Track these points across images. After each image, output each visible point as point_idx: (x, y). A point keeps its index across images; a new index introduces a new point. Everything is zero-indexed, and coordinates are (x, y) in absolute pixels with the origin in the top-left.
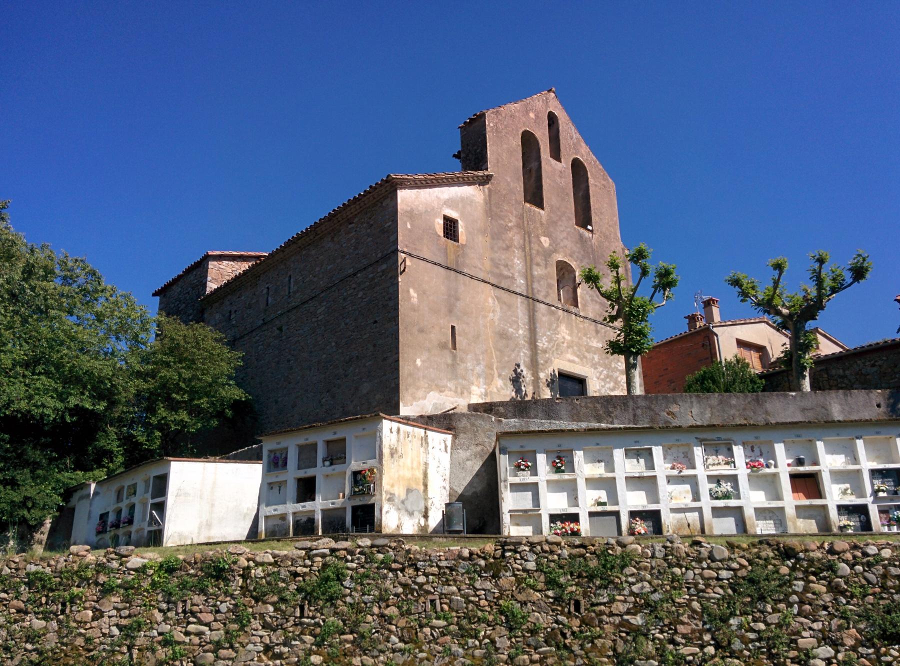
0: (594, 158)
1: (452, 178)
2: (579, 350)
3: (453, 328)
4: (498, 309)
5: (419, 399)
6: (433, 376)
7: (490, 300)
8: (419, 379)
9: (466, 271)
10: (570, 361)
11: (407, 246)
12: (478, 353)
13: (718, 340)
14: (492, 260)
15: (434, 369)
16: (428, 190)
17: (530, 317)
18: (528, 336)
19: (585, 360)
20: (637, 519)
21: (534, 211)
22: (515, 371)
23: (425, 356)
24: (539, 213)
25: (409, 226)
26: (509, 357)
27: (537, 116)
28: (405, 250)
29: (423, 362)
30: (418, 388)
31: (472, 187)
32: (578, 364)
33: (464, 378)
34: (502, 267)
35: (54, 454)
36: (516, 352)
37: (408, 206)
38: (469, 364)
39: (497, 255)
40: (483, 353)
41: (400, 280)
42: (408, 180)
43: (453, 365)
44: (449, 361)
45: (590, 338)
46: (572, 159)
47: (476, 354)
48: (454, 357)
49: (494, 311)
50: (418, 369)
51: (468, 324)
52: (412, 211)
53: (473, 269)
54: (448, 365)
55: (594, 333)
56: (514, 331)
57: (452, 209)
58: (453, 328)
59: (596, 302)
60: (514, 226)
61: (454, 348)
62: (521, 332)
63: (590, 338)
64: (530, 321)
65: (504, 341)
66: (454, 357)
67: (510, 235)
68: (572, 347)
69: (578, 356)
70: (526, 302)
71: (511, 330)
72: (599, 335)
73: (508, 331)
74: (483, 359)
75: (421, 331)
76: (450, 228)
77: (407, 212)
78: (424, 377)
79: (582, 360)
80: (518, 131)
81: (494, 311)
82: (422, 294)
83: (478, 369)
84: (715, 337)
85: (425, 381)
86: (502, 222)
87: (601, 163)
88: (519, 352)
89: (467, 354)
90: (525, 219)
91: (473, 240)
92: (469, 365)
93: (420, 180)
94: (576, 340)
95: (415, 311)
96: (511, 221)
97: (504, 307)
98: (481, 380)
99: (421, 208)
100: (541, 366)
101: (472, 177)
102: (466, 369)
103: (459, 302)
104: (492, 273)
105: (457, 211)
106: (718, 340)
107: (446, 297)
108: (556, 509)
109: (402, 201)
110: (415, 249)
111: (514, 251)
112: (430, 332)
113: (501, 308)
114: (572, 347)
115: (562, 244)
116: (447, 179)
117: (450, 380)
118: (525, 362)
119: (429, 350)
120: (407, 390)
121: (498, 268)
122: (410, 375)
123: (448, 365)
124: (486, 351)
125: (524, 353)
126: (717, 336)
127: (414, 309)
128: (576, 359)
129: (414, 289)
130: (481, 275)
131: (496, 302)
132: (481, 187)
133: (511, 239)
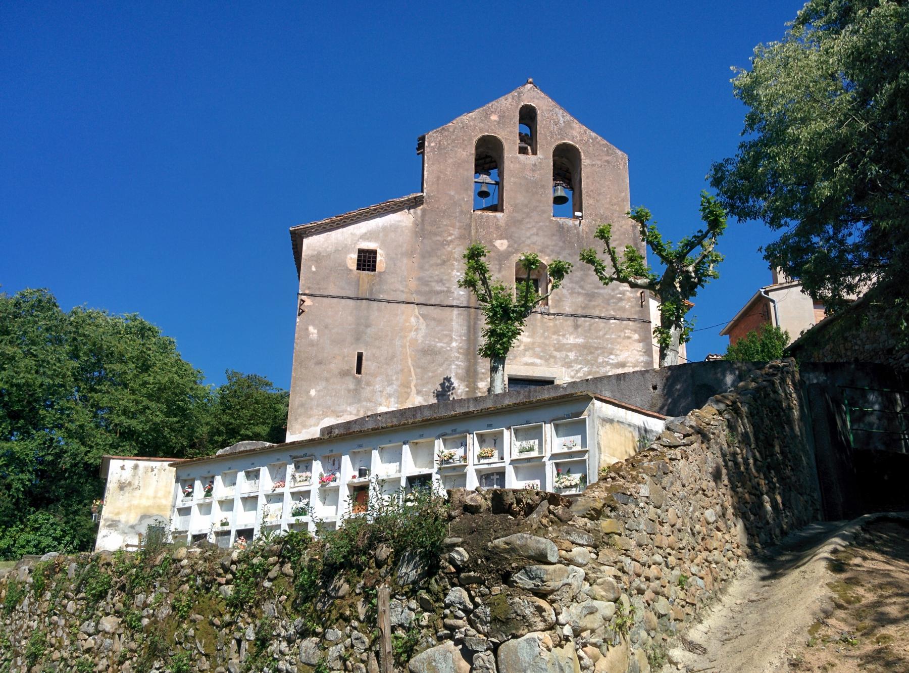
0: (593, 135)
1: (367, 212)
2: (544, 351)
3: (360, 357)
4: (423, 327)
5: (311, 426)
6: (329, 403)
7: (413, 320)
8: (311, 408)
9: (381, 297)
10: (526, 364)
11: (309, 288)
12: (390, 373)
13: (774, 306)
14: (420, 279)
15: (331, 396)
16: (341, 230)
17: (469, 327)
18: (465, 347)
19: (552, 360)
20: (242, 538)
21: (488, 216)
22: (442, 385)
23: (322, 385)
24: (495, 217)
25: (314, 269)
26: (433, 372)
27: (502, 117)
28: (307, 292)
29: (318, 391)
30: (310, 417)
31: (399, 213)
32: (541, 365)
33: (370, 400)
34: (433, 284)
35: (47, 495)
36: (445, 366)
37: (315, 250)
38: (377, 386)
39: (428, 273)
40: (397, 373)
41: (298, 320)
42: (312, 228)
43: (356, 390)
44: (352, 386)
45: (564, 335)
46: (554, 146)
47: (387, 376)
48: (359, 382)
49: (416, 330)
50: (312, 399)
51: (379, 348)
52: (319, 254)
53: (392, 293)
54: (349, 391)
55: (571, 329)
56: (444, 345)
57: (370, 241)
58: (360, 357)
59: (579, 293)
60: (456, 238)
61: (359, 371)
62: (454, 344)
63: (564, 335)
64: (469, 331)
65: (429, 357)
66: (359, 382)
67: (449, 249)
68: (533, 349)
69: (541, 358)
70: (466, 313)
71: (439, 345)
72: (580, 330)
73: (435, 346)
74: (397, 379)
75: (319, 363)
76: (367, 260)
77: (313, 256)
78: (318, 406)
79: (547, 360)
80: (471, 139)
81: (416, 330)
82: (324, 329)
83: (389, 390)
84: (772, 304)
85: (320, 409)
86: (439, 238)
87: (604, 137)
88: (450, 365)
89: (376, 377)
90: (473, 227)
91: (395, 265)
92: (378, 387)
93: (327, 224)
94: (539, 340)
95: (313, 346)
96: (451, 235)
97: (433, 323)
98: (393, 399)
99: (331, 249)
100: (481, 376)
101: (395, 205)
102: (374, 392)
103: (369, 329)
104: (418, 292)
105: (375, 241)
106: (774, 306)
107: (353, 326)
108: (241, 525)
109: (308, 248)
110: (319, 289)
111: (453, 265)
112: (330, 363)
113: (427, 325)
114: (533, 349)
115: (528, 242)
116: (361, 214)
117: (350, 404)
118: (457, 374)
119: (327, 380)
120: (296, 419)
121: (427, 285)
122: (302, 405)
123: (349, 391)
124: (402, 370)
125: (457, 365)
126: (773, 301)
127: (312, 344)
128: (538, 361)
129: (314, 325)
130: (403, 297)
131: (421, 320)
132: (412, 211)
133: (451, 253)
